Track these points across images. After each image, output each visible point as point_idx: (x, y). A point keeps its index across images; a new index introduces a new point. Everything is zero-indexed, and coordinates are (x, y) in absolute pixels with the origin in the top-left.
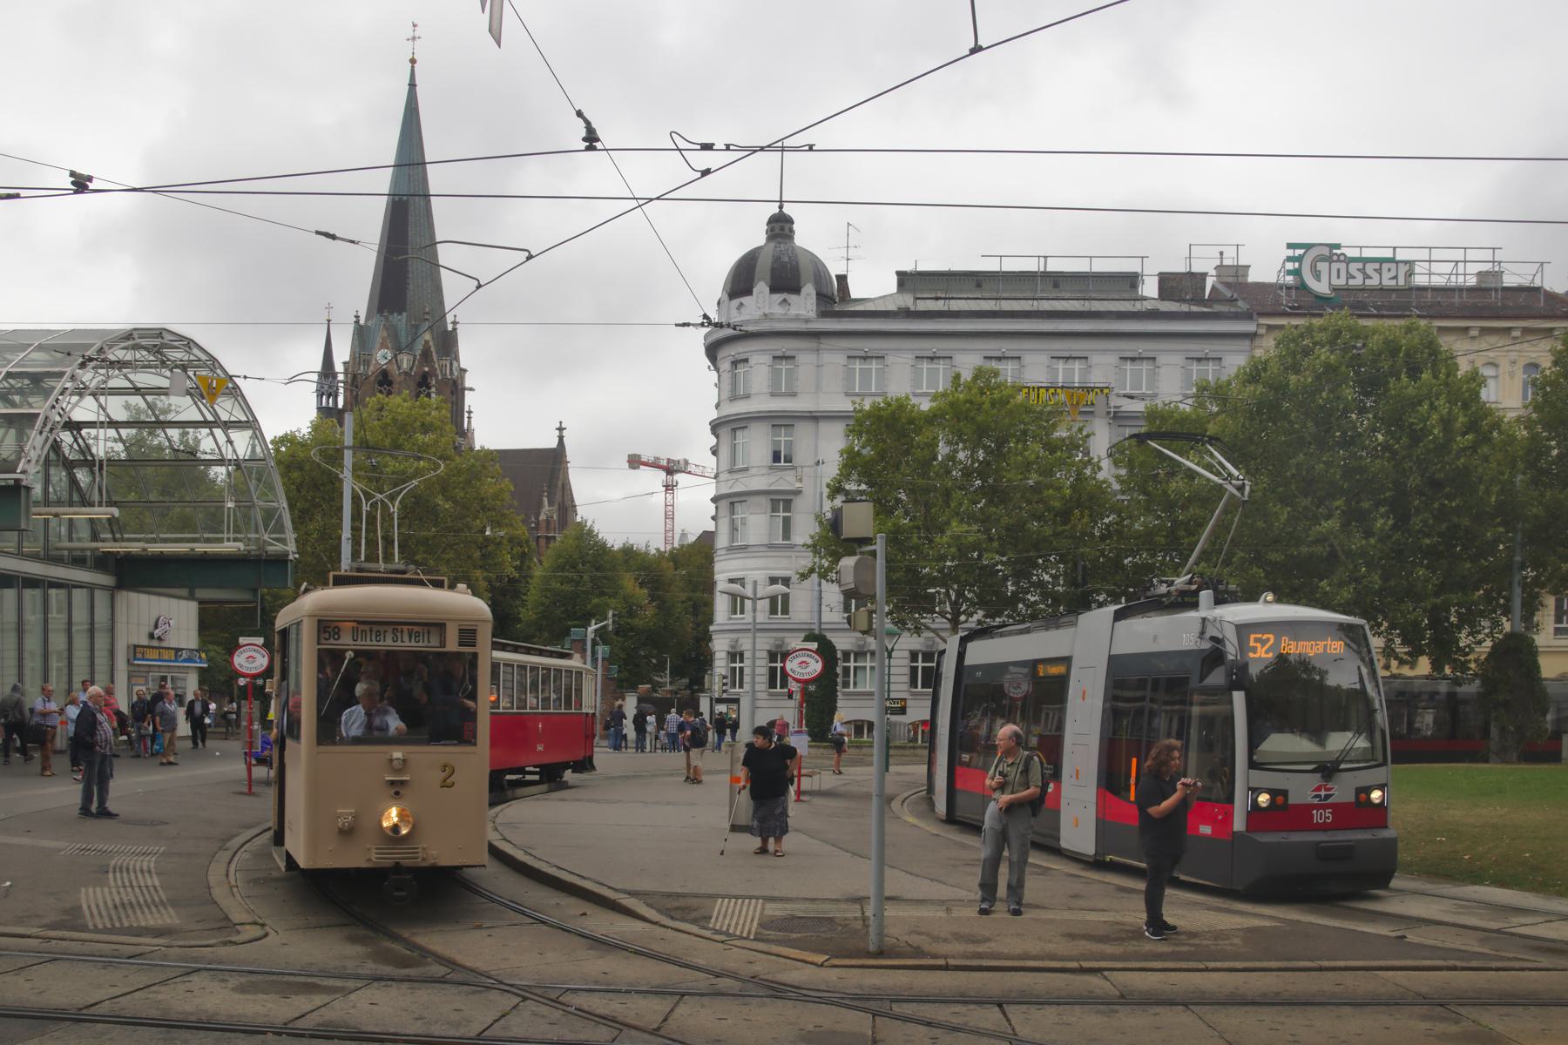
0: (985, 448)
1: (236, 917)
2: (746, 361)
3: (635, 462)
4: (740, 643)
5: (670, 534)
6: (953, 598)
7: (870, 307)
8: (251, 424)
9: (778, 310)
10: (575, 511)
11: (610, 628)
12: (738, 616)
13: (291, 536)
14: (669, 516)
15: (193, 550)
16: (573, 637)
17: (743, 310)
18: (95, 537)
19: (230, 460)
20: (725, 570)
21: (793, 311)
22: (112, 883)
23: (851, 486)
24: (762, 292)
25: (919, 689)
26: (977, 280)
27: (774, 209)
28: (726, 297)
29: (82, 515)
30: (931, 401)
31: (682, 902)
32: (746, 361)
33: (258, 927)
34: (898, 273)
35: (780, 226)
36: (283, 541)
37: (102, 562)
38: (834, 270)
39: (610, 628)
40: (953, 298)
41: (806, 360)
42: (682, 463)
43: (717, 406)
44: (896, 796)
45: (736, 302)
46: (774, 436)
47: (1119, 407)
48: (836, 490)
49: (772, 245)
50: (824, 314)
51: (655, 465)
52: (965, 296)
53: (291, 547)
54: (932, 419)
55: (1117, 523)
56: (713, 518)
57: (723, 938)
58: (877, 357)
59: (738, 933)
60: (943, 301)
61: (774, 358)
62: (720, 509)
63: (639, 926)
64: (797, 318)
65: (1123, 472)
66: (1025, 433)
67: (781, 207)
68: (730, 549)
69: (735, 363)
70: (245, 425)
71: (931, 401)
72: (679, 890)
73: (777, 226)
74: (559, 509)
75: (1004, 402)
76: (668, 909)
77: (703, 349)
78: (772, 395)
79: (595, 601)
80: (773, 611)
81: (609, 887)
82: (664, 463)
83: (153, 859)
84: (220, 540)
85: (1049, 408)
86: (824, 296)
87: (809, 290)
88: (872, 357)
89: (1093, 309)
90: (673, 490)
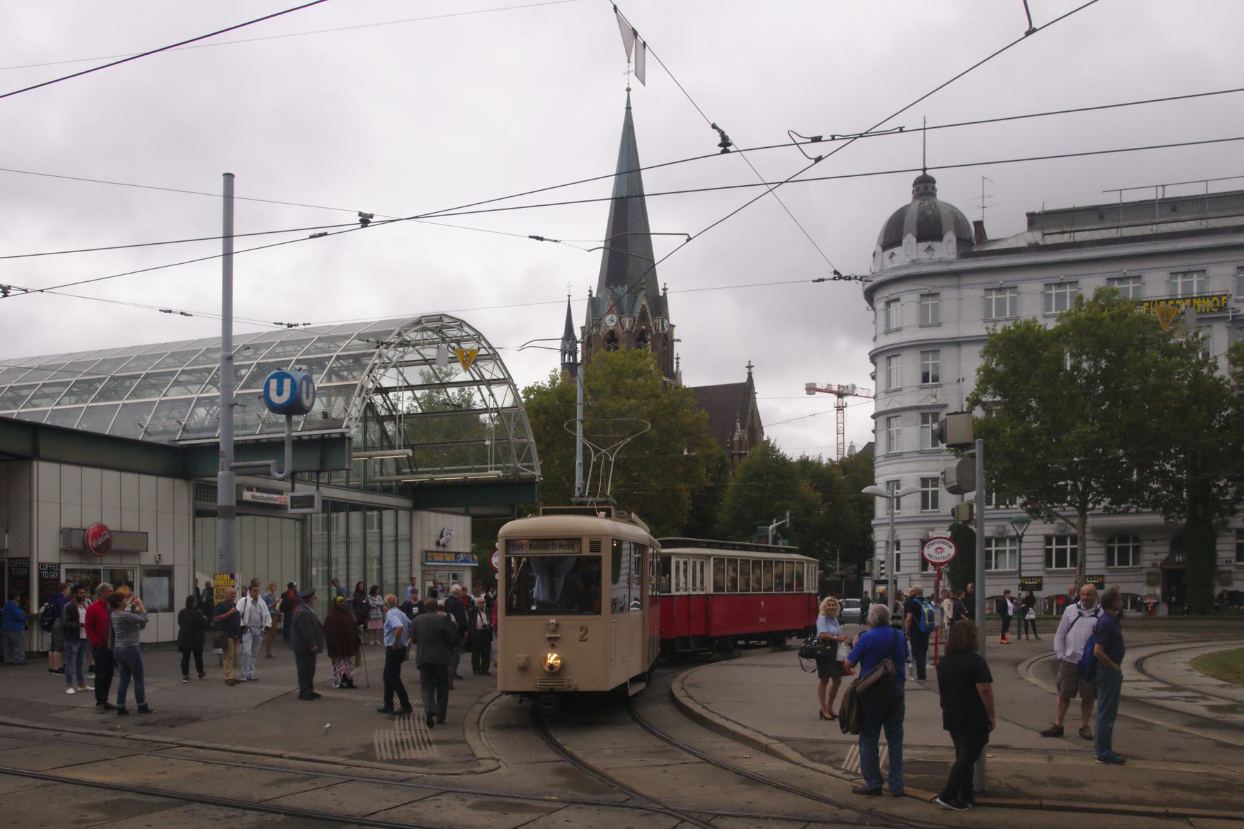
0: (1108, 358)
1: (479, 754)
5: (841, 446)
6: (1081, 488)
8: (507, 381)
9: (924, 256)
11: (788, 525)
13: (537, 463)
14: (840, 431)
15: (466, 478)
18: (399, 472)
19: (492, 409)
20: (883, 473)
24: (909, 243)
25: (1054, 568)
26: (1099, 213)
29: (389, 455)
31: (821, 748)
32: (898, 300)
33: (495, 761)
34: (1028, 215)
36: (532, 468)
37: (404, 490)
38: (971, 218)
39: (788, 525)
40: (1077, 231)
41: (949, 297)
42: (850, 387)
43: (875, 339)
44: (1024, 660)
45: (888, 253)
46: (923, 360)
48: (974, 401)
49: (918, 202)
52: (1088, 228)
53: (538, 472)
54: (1057, 335)
56: (873, 431)
57: (852, 777)
59: (848, 768)
60: (1069, 234)
61: (922, 295)
62: (878, 424)
63: (785, 766)
64: (940, 261)
66: (1143, 341)
68: (888, 456)
69: (888, 303)
70: (502, 381)
72: (821, 737)
74: (750, 430)
75: (1123, 316)
76: (810, 753)
78: (921, 326)
81: (764, 735)
82: (835, 389)
84: (486, 470)
88: (1006, 288)
89: (1210, 227)
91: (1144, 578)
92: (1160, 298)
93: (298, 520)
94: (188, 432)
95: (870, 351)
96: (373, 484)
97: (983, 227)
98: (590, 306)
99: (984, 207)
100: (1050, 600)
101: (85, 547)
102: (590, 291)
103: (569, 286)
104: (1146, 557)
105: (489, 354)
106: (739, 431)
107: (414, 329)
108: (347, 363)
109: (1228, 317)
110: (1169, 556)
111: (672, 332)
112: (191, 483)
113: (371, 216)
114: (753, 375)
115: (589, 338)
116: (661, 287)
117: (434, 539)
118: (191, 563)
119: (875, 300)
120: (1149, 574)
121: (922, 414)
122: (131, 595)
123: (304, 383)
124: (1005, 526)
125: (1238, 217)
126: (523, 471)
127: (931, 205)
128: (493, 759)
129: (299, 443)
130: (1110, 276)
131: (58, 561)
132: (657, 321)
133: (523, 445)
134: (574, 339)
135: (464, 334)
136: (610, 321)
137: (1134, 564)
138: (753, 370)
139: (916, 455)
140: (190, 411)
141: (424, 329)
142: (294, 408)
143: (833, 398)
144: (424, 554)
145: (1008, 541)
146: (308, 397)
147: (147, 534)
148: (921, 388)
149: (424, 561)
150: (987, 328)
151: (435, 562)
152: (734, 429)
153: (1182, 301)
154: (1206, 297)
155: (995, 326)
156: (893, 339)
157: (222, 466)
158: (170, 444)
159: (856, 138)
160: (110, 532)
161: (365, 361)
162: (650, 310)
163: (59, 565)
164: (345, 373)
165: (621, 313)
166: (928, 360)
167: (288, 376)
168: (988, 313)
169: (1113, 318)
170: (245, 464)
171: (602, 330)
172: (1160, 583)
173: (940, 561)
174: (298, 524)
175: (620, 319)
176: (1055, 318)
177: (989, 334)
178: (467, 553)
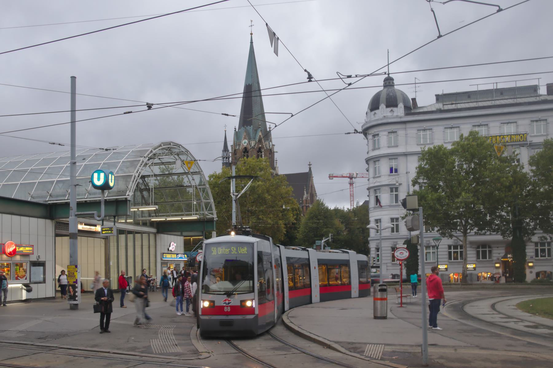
0: (475, 163)
2: (378, 135)
6: (464, 223)
9: (389, 114)
10: (316, 196)
13: (215, 212)
16: (317, 244)
17: (376, 115)
19: (194, 186)
20: (373, 215)
21: (395, 114)
23: (421, 181)
24: (383, 108)
25: (453, 260)
27: (387, 76)
28: (369, 111)
30: (452, 146)
34: (437, 95)
35: (389, 82)
36: (212, 214)
38: (410, 96)
41: (401, 133)
43: (368, 153)
45: (373, 112)
47: (532, 141)
48: (415, 182)
49: (386, 89)
50: (407, 114)
52: (464, 102)
53: (215, 216)
54: (453, 152)
55: (532, 190)
56: (368, 196)
58: (429, 129)
61: (389, 133)
62: (370, 192)
64: (397, 117)
65: (534, 168)
68: (374, 208)
69: (374, 136)
70: (198, 173)
71: (452, 146)
73: (387, 82)
75: (482, 144)
78: (389, 147)
79: (325, 230)
82: (348, 175)
84: (191, 215)
87: (401, 105)
88: (427, 130)
89: (518, 102)
90: (353, 185)
92: (497, 135)
93: (103, 239)
95: (366, 158)
97: (416, 101)
98: (235, 136)
102: (235, 128)
103: (226, 126)
109: (527, 144)
111: (273, 148)
112: (54, 221)
114: (312, 169)
115: (235, 150)
118: (54, 260)
122: (25, 276)
125: (531, 98)
126: (207, 215)
127: (392, 91)
128: (207, 352)
129: (107, 202)
132: (266, 143)
134: (228, 151)
136: (245, 143)
138: (311, 166)
139: (388, 207)
140: (53, 188)
144: (162, 254)
146: (112, 182)
147: (33, 246)
148: (389, 175)
150: (421, 148)
152: (303, 194)
153: (506, 136)
158: (44, 203)
165: (250, 139)
166: (393, 163)
169: (477, 145)
170: (82, 213)
171: (241, 147)
175: (249, 142)
176: (451, 144)
177: (422, 151)
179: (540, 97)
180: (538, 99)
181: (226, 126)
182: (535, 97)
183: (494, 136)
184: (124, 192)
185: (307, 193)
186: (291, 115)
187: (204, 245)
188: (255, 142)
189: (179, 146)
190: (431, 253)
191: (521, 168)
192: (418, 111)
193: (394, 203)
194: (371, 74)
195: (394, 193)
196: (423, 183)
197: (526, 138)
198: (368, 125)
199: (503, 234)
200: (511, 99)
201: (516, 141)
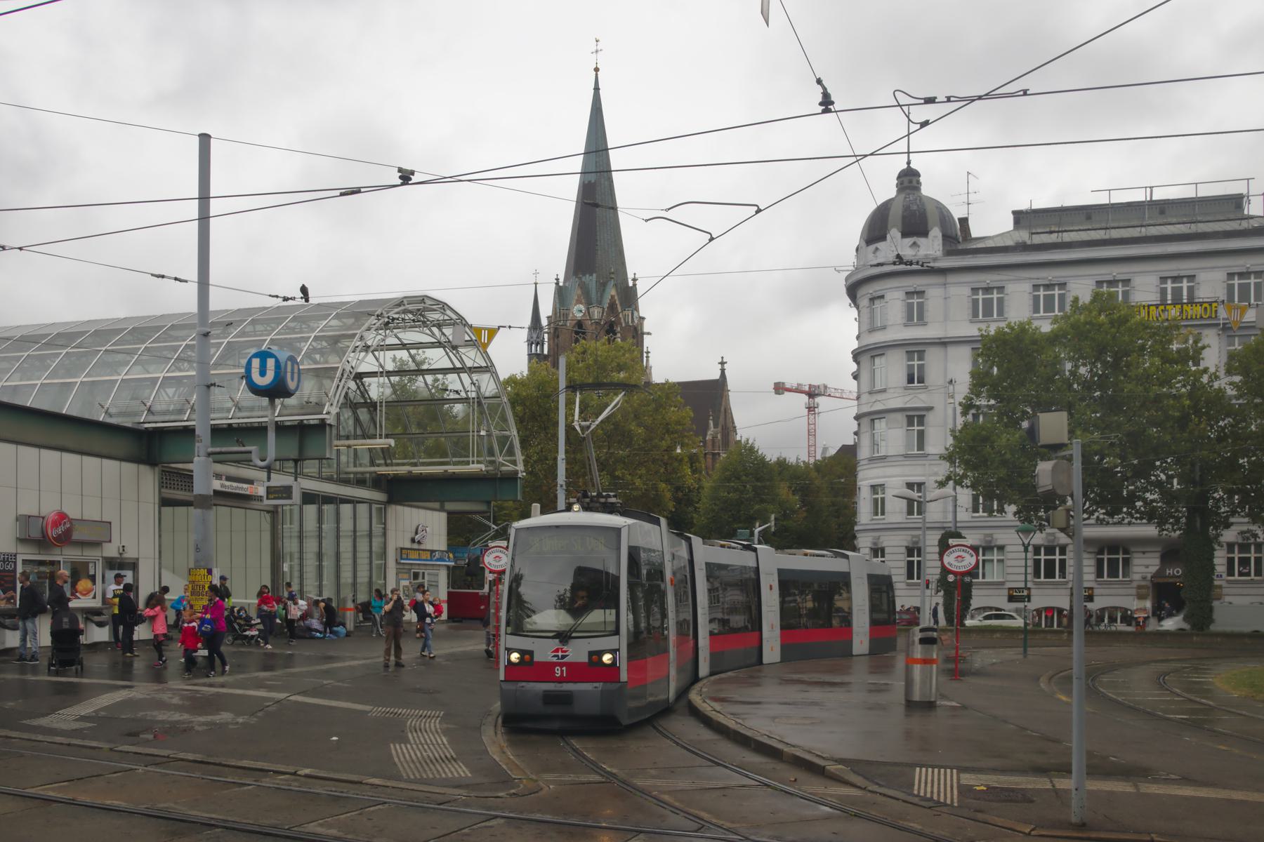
0: (1105, 363)
2: (882, 297)
3: (780, 388)
4: (881, 540)
7: (990, 244)
8: (489, 368)
10: (736, 431)
12: (880, 517)
13: (519, 457)
14: (812, 433)
15: (446, 471)
17: (878, 253)
18: (372, 464)
19: (473, 398)
20: (866, 477)
22: (412, 742)
23: (982, 402)
26: (1087, 213)
28: (864, 244)
29: (363, 445)
30: (1052, 324)
32: (882, 297)
34: (1014, 213)
35: (909, 179)
36: (514, 463)
37: (378, 482)
38: (957, 213)
39: (773, 529)
41: (935, 293)
43: (858, 338)
45: (872, 247)
46: (909, 360)
48: (967, 407)
49: (903, 196)
50: (949, 253)
51: (798, 390)
52: (1076, 228)
53: (520, 467)
54: (1053, 339)
55: (1232, 426)
56: (856, 433)
60: (1056, 234)
61: (907, 293)
65: (1237, 379)
66: (1143, 348)
67: (909, 163)
69: (872, 300)
71: (1052, 324)
73: (906, 180)
75: (1124, 320)
77: (844, 290)
78: (906, 325)
79: (757, 507)
80: (910, 512)
82: (807, 388)
83: (438, 721)
84: (468, 463)
85: (1166, 324)
86: (950, 237)
87: (936, 233)
89: (1200, 231)
91: (1134, 591)
92: (1150, 303)
93: (268, 512)
94: (153, 413)
96: (345, 476)
97: (968, 225)
98: (557, 296)
99: (968, 204)
100: (1039, 611)
101: (44, 537)
102: (557, 279)
103: (536, 273)
104: (1135, 569)
105: (471, 340)
106: (712, 429)
107: (396, 310)
108: (319, 347)
109: (1219, 324)
110: (1159, 569)
111: (642, 325)
112: (157, 469)
113: (412, 173)
115: (556, 329)
116: (630, 276)
117: (409, 535)
119: (858, 296)
120: (1139, 587)
121: (907, 416)
122: (91, 590)
123: (289, 363)
124: (992, 534)
125: (1228, 222)
126: (503, 465)
129: (281, 429)
130: (1100, 279)
131: (14, 552)
132: (626, 312)
133: (507, 437)
134: (541, 328)
135: (446, 318)
136: (578, 311)
137: (1123, 577)
139: (902, 458)
141: (405, 312)
142: (277, 391)
143: (805, 398)
144: (399, 551)
145: (995, 549)
146: (292, 379)
147: (110, 523)
148: (906, 388)
149: (399, 559)
151: (410, 560)
152: (706, 428)
154: (1196, 303)
155: (988, 327)
156: (879, 337)
157: (198, 452)
158: (136, 426)
159: (973, 100)
160: (71, 521)
161: (346, 343)
162: (619, 299)
163: (15, 556)
164: (318, 357)
165: (589, 304)
167: (272, 355)
168: (975, 314)
170: (224, 449)
172: (1150, 597)
173: (961, 570)
174: (268, 516)
175: (588, 309)
178: (443, 551)
179: (1251, 221)
180: (1245, 225)
181: (536, 273)
182: (1239, 222)
183: (1144, 306)
184: (319, 406)
185: (716, 426)
186: (756, 208)
187: (512, 532)
188: (601, 310)
189: (444, 306)
190: (995, 561)
191: (1213, 377)
192: (975, 247)
193: (914, 450)
194: (986, 95)
195: (916, 428)
196: (988, 406)
197: (1216, 311)
198: (860, 276)
199: (1160, 524)
200: (1184, 223)
201: (1194, 317)
